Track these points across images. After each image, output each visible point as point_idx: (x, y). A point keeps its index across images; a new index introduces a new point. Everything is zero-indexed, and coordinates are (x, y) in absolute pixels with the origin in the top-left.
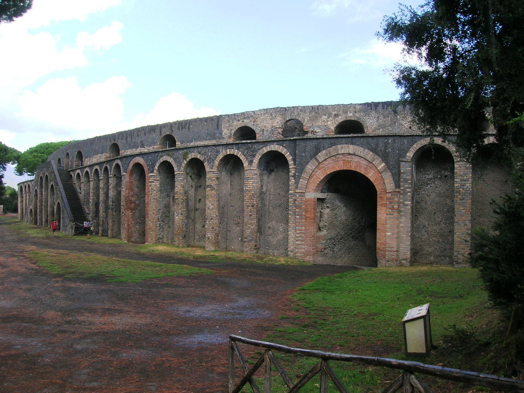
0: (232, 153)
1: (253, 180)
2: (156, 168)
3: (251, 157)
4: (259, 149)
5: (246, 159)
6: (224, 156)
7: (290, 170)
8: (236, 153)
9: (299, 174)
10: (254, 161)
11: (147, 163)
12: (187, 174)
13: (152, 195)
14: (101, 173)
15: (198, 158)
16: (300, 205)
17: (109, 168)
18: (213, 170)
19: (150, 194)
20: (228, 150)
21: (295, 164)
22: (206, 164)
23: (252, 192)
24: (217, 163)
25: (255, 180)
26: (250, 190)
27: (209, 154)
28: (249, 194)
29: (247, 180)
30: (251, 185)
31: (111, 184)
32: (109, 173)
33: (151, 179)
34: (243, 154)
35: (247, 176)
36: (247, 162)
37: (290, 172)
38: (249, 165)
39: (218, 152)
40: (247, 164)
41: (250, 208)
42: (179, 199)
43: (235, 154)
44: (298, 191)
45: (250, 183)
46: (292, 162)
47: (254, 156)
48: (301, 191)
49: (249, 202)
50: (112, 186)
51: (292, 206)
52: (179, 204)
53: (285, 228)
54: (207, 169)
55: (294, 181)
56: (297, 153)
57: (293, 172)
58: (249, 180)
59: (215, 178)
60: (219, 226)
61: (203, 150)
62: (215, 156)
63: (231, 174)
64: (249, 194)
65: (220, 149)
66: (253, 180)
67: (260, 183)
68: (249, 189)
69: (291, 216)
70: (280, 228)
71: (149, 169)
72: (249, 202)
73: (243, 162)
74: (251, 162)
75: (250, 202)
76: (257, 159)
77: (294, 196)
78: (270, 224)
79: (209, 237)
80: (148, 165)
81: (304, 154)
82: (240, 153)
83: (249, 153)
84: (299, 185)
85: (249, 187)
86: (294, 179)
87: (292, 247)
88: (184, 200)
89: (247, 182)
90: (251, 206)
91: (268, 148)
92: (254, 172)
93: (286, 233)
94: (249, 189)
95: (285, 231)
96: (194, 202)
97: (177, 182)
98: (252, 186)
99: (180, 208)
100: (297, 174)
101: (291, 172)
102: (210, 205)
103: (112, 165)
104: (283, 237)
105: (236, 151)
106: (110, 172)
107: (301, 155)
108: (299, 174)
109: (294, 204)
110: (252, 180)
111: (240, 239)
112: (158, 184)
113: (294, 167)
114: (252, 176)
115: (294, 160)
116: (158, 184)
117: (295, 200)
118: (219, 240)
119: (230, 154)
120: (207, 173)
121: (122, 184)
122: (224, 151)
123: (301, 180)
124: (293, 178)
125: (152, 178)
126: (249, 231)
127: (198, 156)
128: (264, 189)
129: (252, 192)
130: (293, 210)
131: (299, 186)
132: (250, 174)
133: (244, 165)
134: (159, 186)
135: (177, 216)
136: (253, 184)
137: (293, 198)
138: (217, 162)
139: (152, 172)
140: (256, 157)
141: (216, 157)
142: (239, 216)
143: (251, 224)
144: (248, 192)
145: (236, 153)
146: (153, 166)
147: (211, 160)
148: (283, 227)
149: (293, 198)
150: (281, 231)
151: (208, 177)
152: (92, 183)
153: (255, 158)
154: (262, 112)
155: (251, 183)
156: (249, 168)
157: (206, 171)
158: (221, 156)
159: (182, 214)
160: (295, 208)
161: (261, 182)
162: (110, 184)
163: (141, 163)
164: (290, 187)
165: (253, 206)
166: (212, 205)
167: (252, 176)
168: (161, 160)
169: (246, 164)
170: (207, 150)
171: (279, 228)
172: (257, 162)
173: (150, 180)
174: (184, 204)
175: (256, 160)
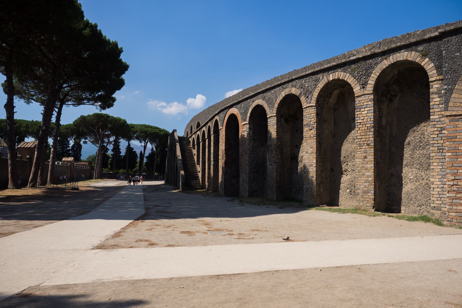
0: (336, 78)
1: (369, 109)
2: (249, 115)
3: (364, 77)
4: (376, 64)
5: (356, 82)
6: (325, 83)
7: (431, 84)
8: (342, 76)
9: (450, 87)
10: (370, 82)
11: (240, 112)
12: (282, 116)
13: (246, 145)
14: (206, 132)
15: (293, 93)
16: (452, 135)
17: (211, 126)
18: (311, 105)
19: (243, 144)
20: (331, 75)
21: (439, 74)
22: (303, 99)
23: (367, 125)
24: (317, 94)
25: (371, 108)
26: (363, 123)
27: (306, 86)
28: (363, 128)
29: (358, 110)
30: (365, 115)
31: (212, 140)
32: (211, 131)
33: (244, 128)
34: (353, 76)
35: (359, 105)
36: (358, 85)
37: (430, 87)
38: (361, 88)
39: (317, 81)
40: (359, 88)
41: (364, 147)
42: (272, 145)
43: (341, 78)
44: (448, 113)
45: (363, 113)
46: (435, 71)
47: (369, 75)
48: (454, 113)
49: (362, 140)
50: (213, 143)
51: (435, 139)
52: (272, 151)
53: (418, 175)
54: (304, 105)
55: (438, 99)
56: (444, 55)
57: (435, 86)
58: (362, 110)
59: (314, 115)
60: (321, 174)
61: (298, 83)
62: (313, 87)
63: (335, 110)
64: (363, 128)
65: (320, 76)
66: (369, 109)
67: (377, 113)
68: (362, 121)
69: (435, 154)
70: (410, 175)
71: (242, 118)
72: (362, 140)
73: (352, 86)
74: (364, 86)
75: (364, 140)
76: (373, 79)
77: (439, 123)
78: (393, 169)
79: (308, 188)
80: (241, 114)
81: (458, 54)
82: (348, 75)
83: (361, 73)
84: (450, 104)
85: (362, 118)
86: (439, 97)
87: (437, 202)
88: (278, 146)
89: (359, 113)
90: (365, 145)
91: (391, 60)
92: (370, 97)
93: (419, 182)
94: (362, 121)
95: (418, 179)
96: (289, 148)
97: (270, 126)
98: (367, 118)
99: (273, 155)
100: (446, 87)
101: (432, 88)
102: (309, 148)
103: (213, 122)
104: (415, 188)
105: (342, 73)
106: (212, 130)
107: (452, 56)
108: (450, 87)
109: (439, 135)
110: (366, 109)
111: (348, 191)
112: (251, 132)
113: (438, 78)
114: (366, 103)
115: (439, 68)
116: (251, 132)
117: (442, 129)
118: (321, 192)
119: (334, 80)
120: (304, 110)
121: (220, 138)
122: (325, 78)
123: (453, 95)
124: (436, 96)
125: (245, 127)
126: (363, 179)
127: (294, 91)
128: (384, 121)
129: (367, 125)
130: (438, 145)
131: (450, 105)
132: (363, 101)
133: (354, 90)
134: (252, 134)
135: (271, 165)
136: (368, 115)
137: (437, 126)
138: (316, 94)
139: (245, 120)
140: (372, 75)
141: (315, 88)
142: (347, 162)
143: (366, 169)
144: (361, 126)
145: (342, 76)
146: (246, 113)
147: (308, 93)
148: (415, 173)
149: (437, 126)
150: (410, 180)
151: (306, 114)
152: (201, 144)
153: (371, 78)
154: (368, 48)
155: (366, 112)
156: (362, 93)
157: (303, 107)
158: (321, 85)
159: (276, 163)
160: (442, 142)
161: (379, 111)
162: (212, 141)
163: (235, 113)
164: (431, 111)
165: (368, 145)
166: (311, 148)
167: (366, 103)
168: (254, 105)
169: (357, 89)
170: (304, 82)
171: (407, 175)
172: (373, 83)
173: (243, 130)
174: (278, 151)
175: (372, 82)
